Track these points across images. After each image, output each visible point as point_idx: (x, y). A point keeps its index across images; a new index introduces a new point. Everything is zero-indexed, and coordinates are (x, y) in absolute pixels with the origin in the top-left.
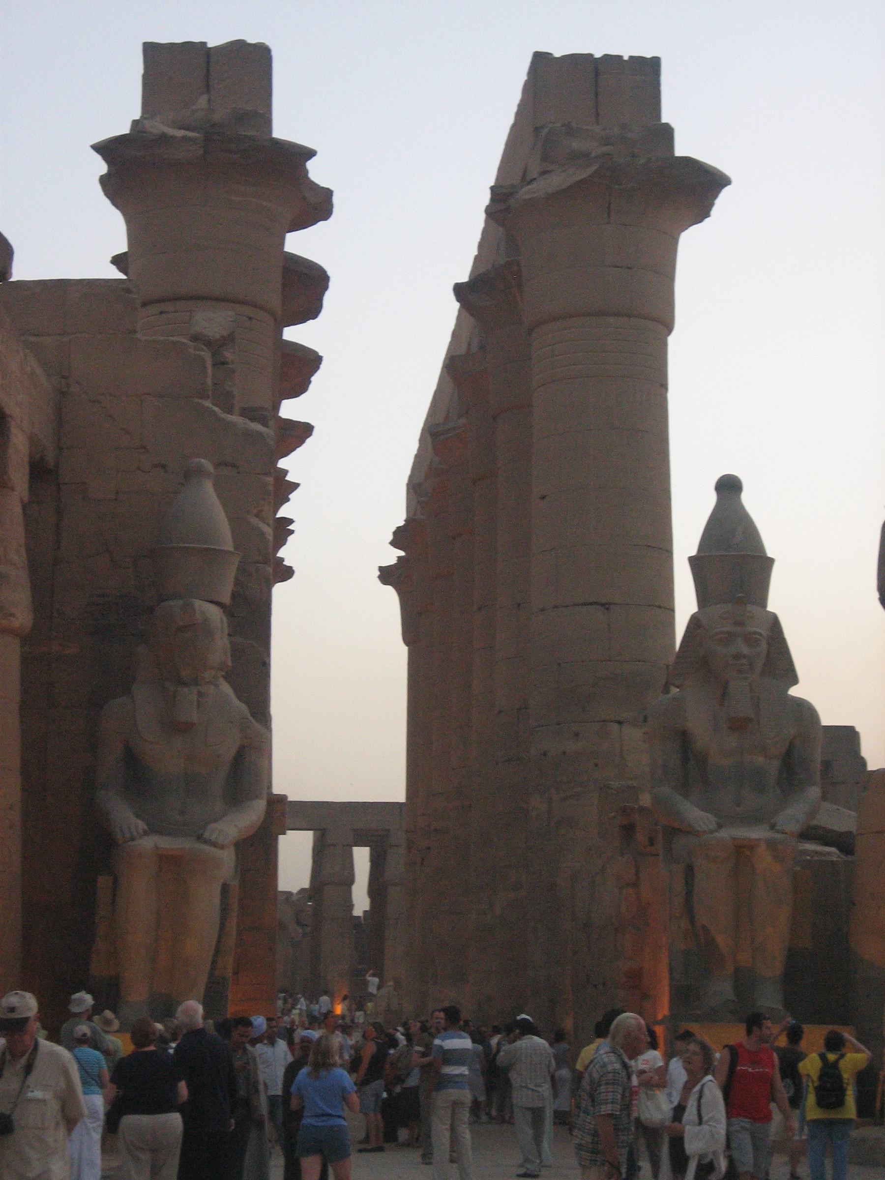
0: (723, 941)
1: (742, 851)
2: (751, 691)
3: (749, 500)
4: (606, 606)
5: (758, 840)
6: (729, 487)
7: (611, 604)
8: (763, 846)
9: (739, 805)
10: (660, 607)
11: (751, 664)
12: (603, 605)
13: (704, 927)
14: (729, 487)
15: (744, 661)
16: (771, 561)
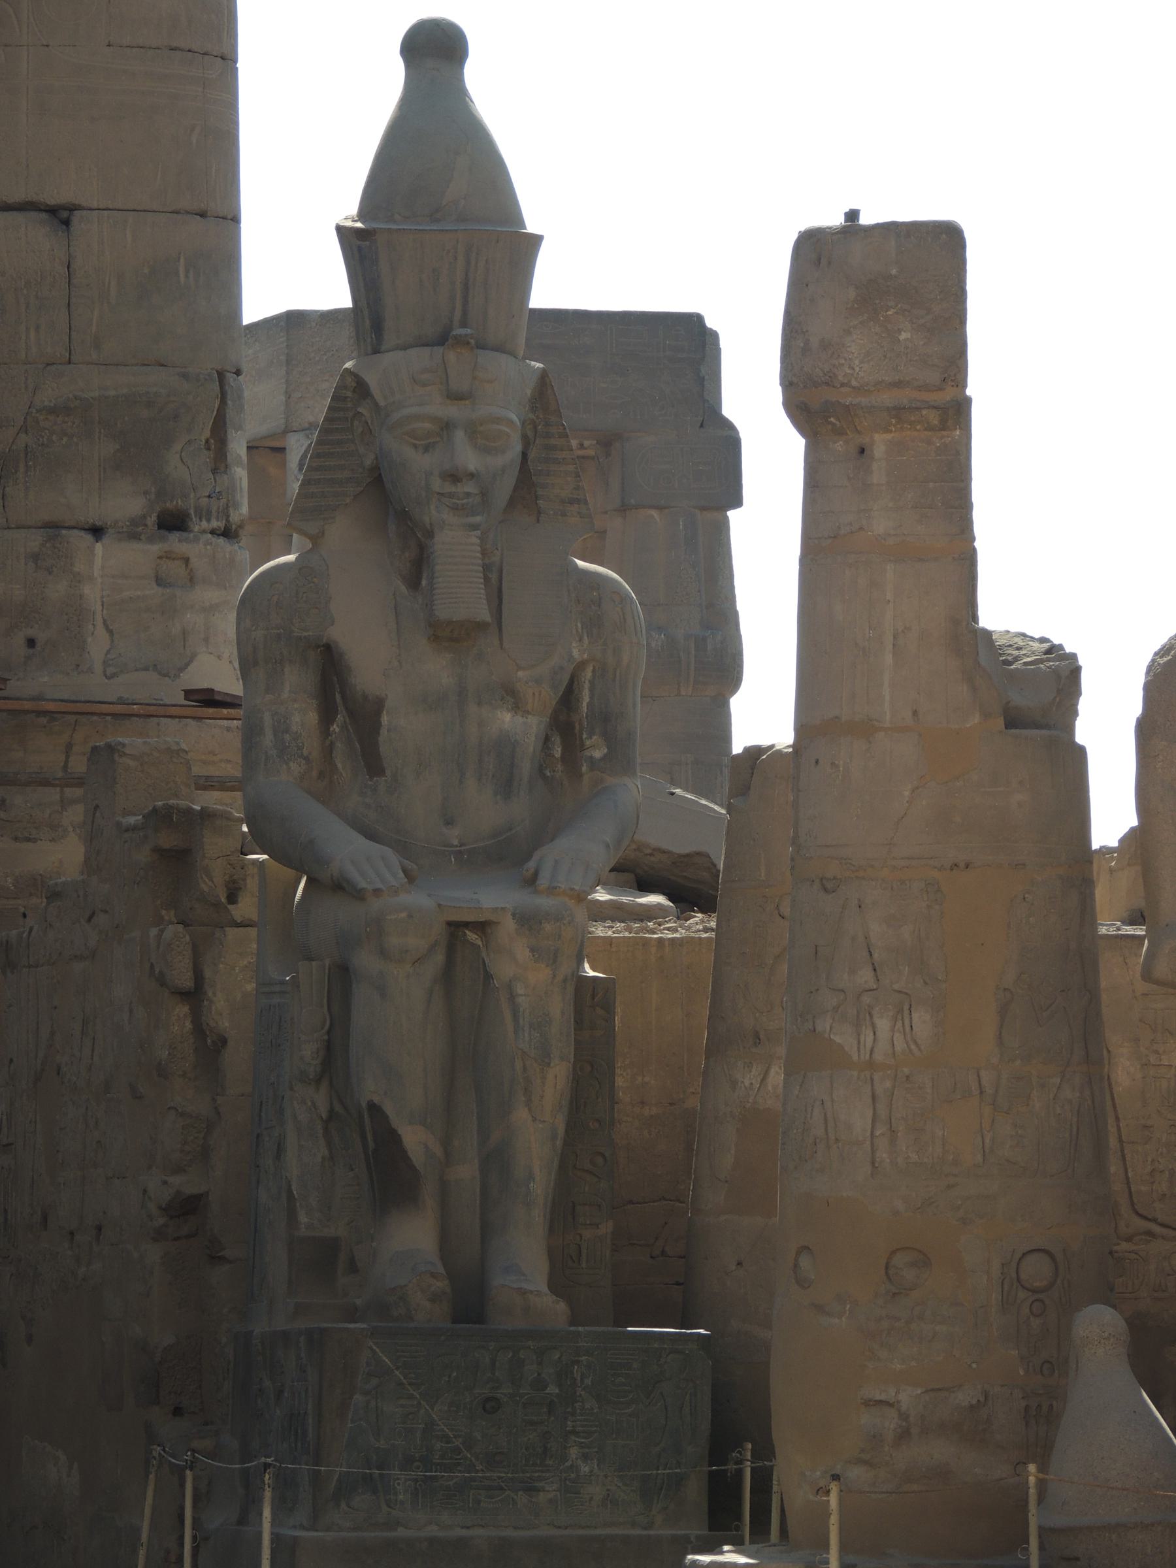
0: (415, 1140)
1: (462, 936)
2: (484, 553)
3: (486, 84)
4: (61, 216)
5: (495, 910)
6: (434, 51)
7: (73, 208)
8: (509, 924)
9: (449, 822)
10: (203, 215)
11: (484, 494)
12: (52, 211)
13: (374, 1108)
14: (434, 51)
15: (470, 487)
16: (535, 241)
